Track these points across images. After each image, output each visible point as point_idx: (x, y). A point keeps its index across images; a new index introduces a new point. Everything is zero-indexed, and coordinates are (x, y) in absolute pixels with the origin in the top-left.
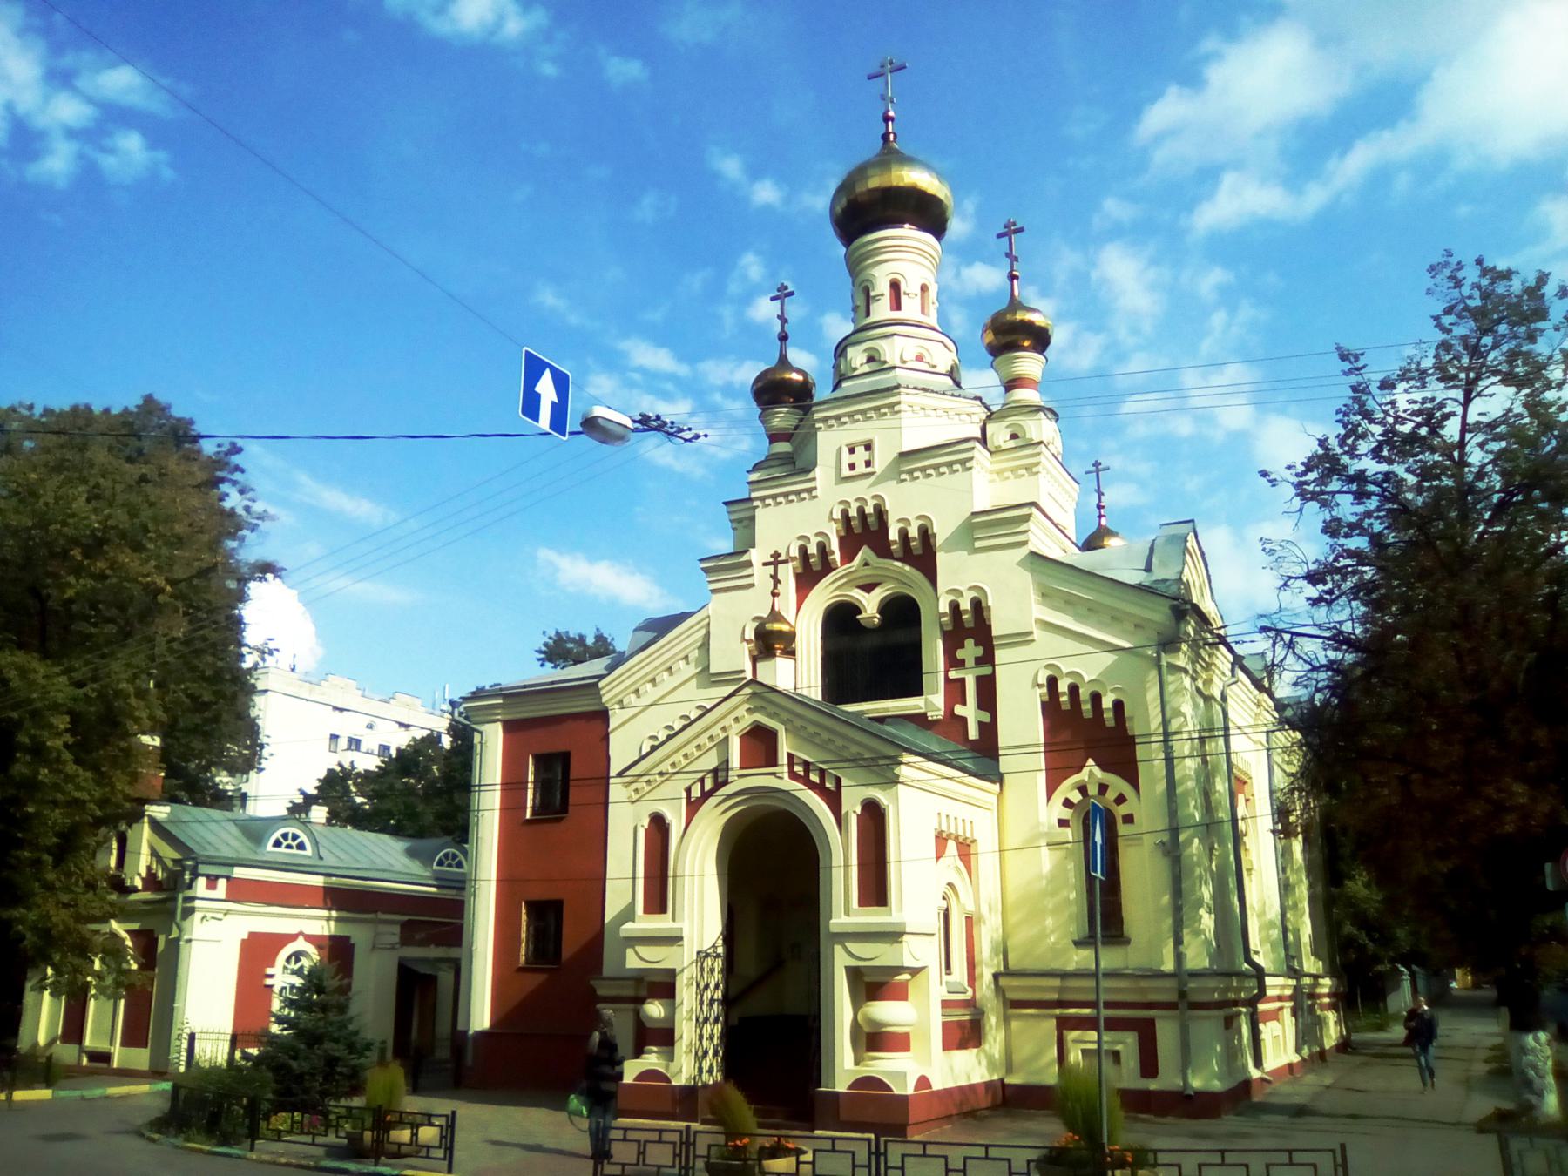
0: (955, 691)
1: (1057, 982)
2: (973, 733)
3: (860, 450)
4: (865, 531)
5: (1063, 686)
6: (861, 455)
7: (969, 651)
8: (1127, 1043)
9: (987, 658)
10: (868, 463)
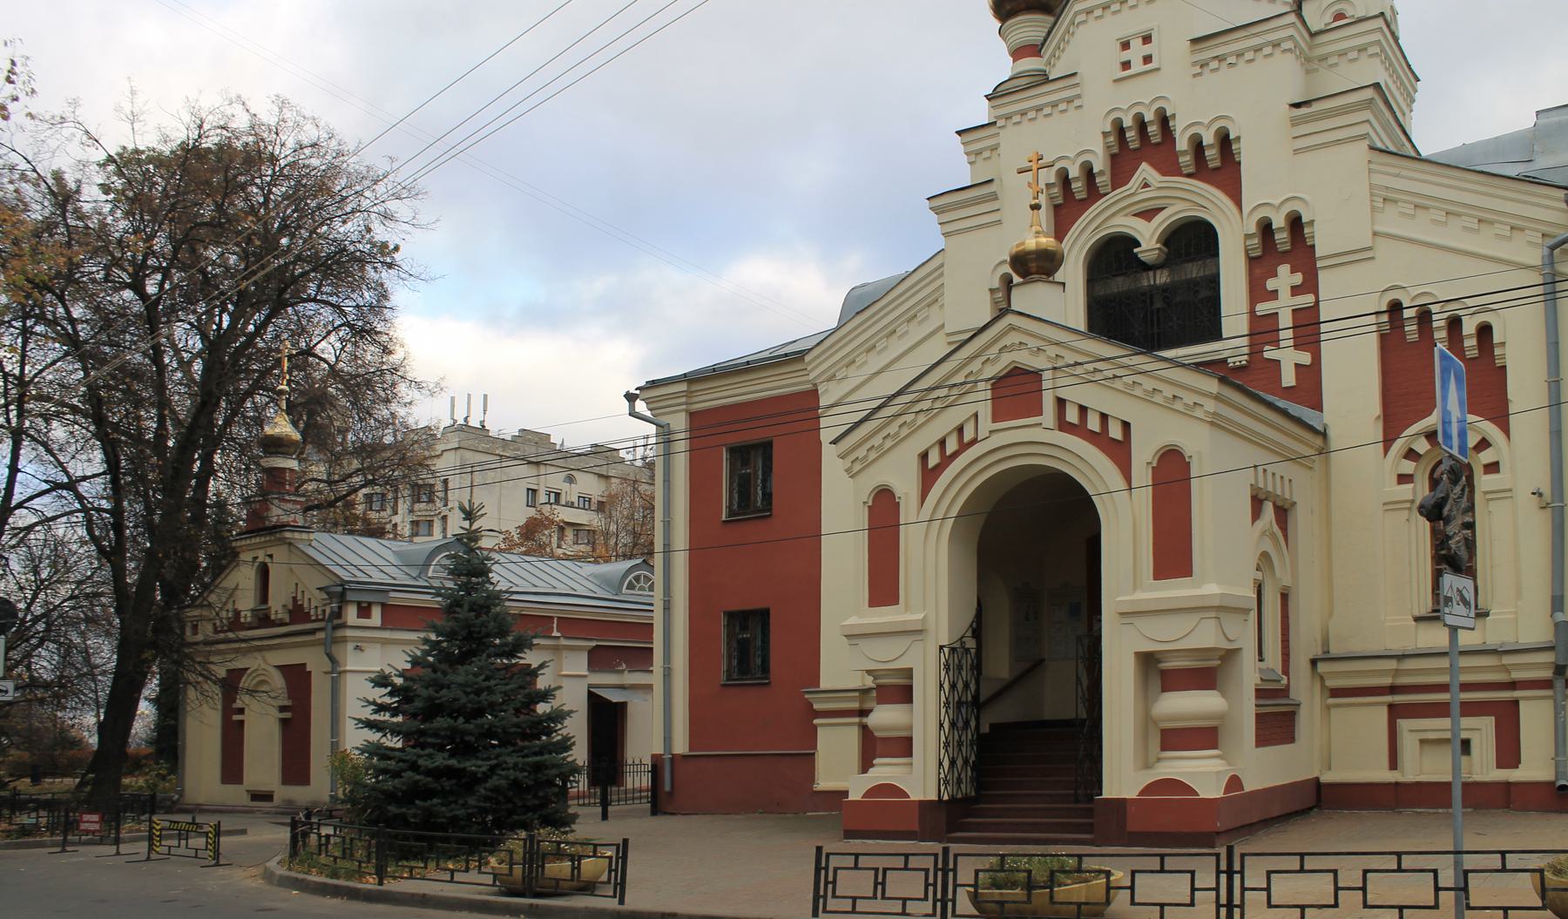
3: (1136, 44)
4: (1143, 143)
10: (1147, 59)
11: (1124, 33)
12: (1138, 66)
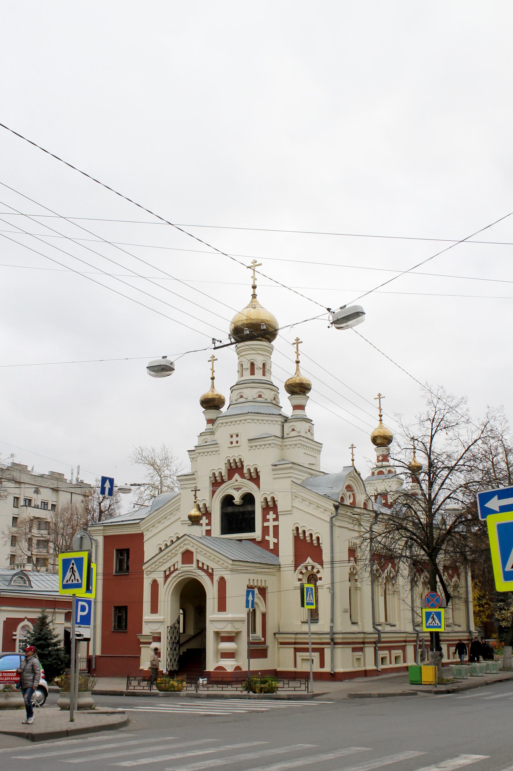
0: (265, 530)
1: (294, 636)
2: (272, 547)
3: (234, 436)
4: (235, 469)
5: (300, 531)
6: (235, 439)
7: (271, 516)
8: (316, 656)
9: (276, 519)
10: (237, 442)
11: (232, 432)
12: (234, 444)
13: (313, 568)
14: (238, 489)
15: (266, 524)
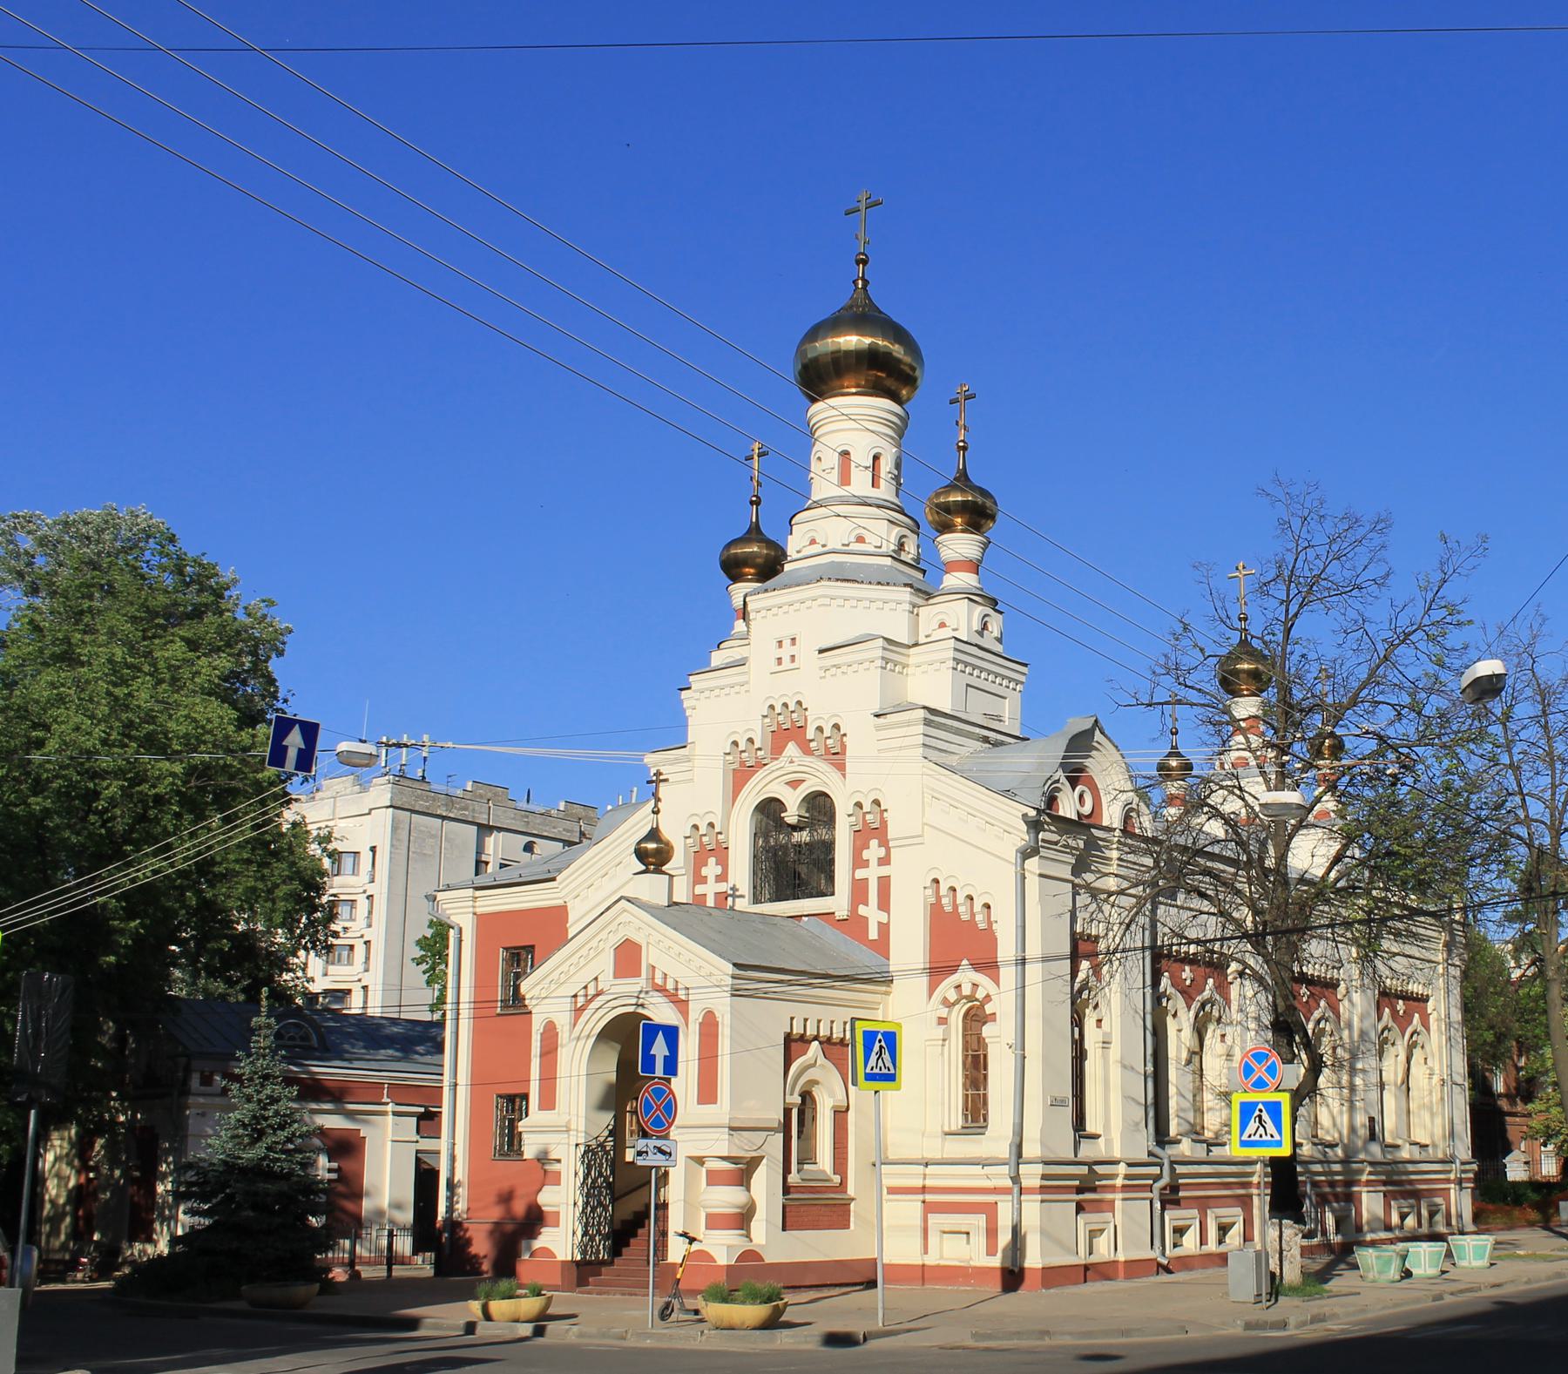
0: (859, 891)
2: (873, 934)
3: (786, 643)
4: (788, 731)
5: (943, 890)
7: (873, 852)
12: (786, 663)
13: (975, 986)
14: (794, 784)
15: (860, 874)
